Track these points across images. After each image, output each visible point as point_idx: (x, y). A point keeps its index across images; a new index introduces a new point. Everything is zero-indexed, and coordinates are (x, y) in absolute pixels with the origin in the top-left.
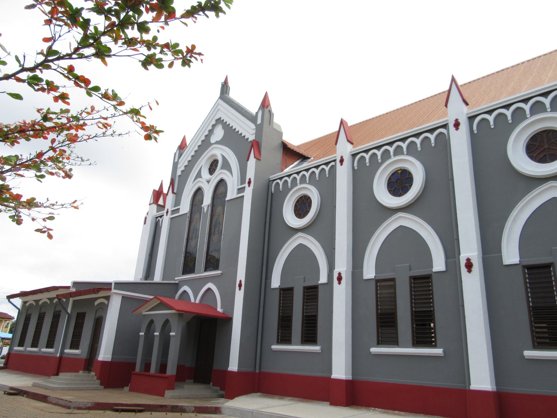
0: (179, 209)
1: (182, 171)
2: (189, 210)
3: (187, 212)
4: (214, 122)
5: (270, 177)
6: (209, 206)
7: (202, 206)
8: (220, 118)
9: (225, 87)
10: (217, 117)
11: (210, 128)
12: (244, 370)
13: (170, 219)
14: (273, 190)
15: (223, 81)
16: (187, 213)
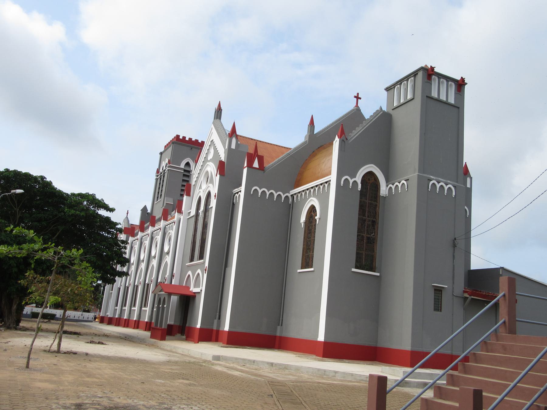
0: (190, 212)
1: (196, 181)
2: (194, 213)
3: (193, 215)
4: (209, 144)
5: (233, 191)
6: (202, 212)
7: (200, 211)
8: (213, 140)
9: (219, 112)
10: (211, 140)
11: (208, 148)
12: (205, 327)
13: (187, 220)
14: (234, 201)
15: (216, 106)
16: (193, 216)
